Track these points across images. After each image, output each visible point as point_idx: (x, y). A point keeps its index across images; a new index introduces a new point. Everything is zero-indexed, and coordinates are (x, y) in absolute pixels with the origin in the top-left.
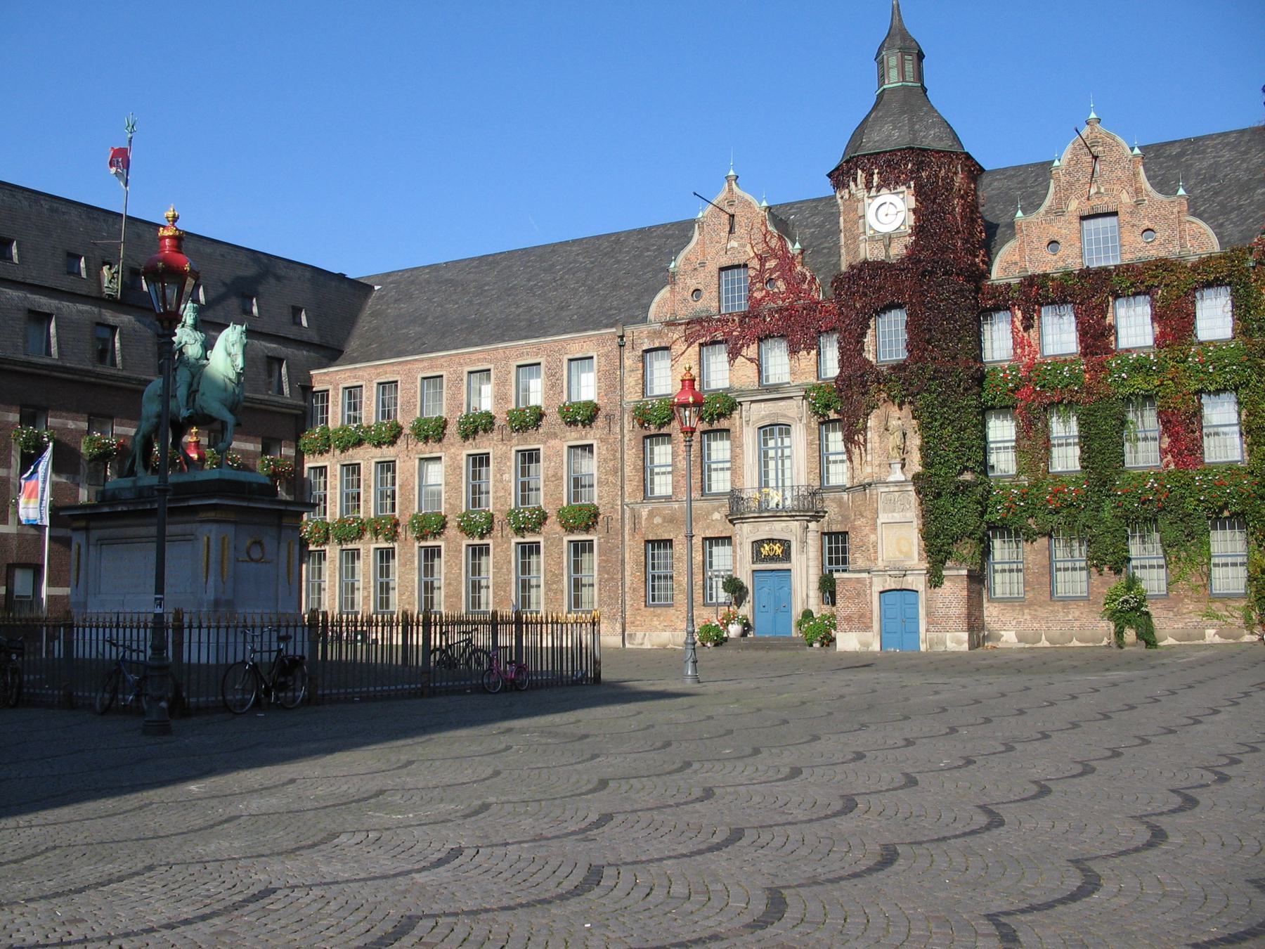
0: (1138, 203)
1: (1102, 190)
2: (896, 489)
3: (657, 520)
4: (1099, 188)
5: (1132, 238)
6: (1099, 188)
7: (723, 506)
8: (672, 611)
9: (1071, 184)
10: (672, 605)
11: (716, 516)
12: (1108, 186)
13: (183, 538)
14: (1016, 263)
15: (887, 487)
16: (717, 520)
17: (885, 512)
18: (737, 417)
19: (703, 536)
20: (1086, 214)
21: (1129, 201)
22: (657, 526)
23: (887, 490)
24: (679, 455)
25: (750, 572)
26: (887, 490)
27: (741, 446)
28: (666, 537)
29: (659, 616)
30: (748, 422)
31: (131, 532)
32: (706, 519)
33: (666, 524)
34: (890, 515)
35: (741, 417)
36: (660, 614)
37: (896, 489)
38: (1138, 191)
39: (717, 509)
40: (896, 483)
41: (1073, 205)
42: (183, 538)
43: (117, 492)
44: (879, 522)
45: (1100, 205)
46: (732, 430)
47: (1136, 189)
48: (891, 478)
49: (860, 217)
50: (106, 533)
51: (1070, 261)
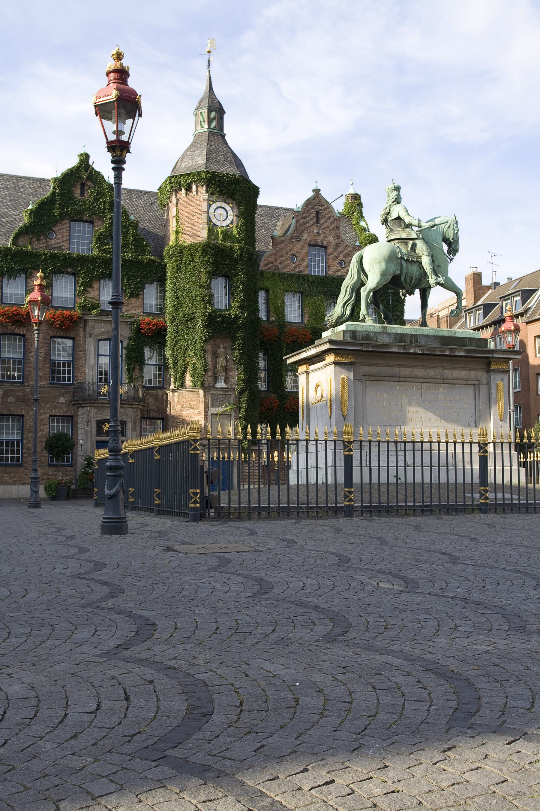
0: (338, 245)
1: (320, 232)
2: (221, 393)
3: (11, 399)
4: (319, 230)
5: (334, 263)
6: (319, 230)
7: (68, 393)
8: (21, 469)
9: (305, 224)
10: (21, 465)
11: (62, 400)
12: (323, 230)
13: (465, 382)
14: (273, 263)
15: (216, 391)
16: (62, 403)
17: (213, 406)
18: (82, 330)
19: (51, 414)
20: (312, 243)
21: (333, 241)
22: (11, 403)
23: (215, 393)
24: (31, 352)
25: (95, 443)
26: (215, 393)
27: (84, 351)
28: (18, 412)
29: (10, 473)
30: (90, 335)
31: (406, 371)
32: (53, 402)
33: (18, 403)
34: (217, 409)
35: (85, 331)
36: (11, 472)
37: (221, 393)
38: (338, 238)
39: (63, 395)
40: (222, 389)
41: (305, 236)
42: (465, 382)
43: (372, 335)
44: (210, 413)
45: (321, 239)
46: (77, 338)
47: (337, 236)
48: (218, 385)
49: (204, 212)
50: (375, 370)
51: (302, 268)
